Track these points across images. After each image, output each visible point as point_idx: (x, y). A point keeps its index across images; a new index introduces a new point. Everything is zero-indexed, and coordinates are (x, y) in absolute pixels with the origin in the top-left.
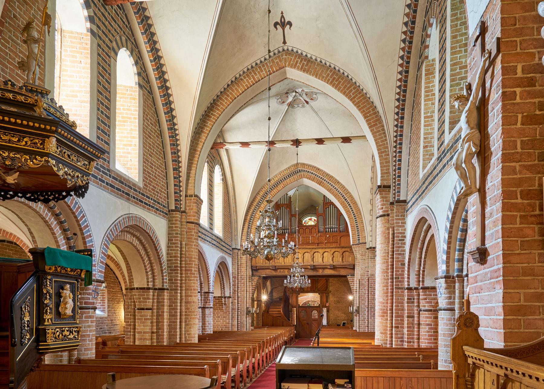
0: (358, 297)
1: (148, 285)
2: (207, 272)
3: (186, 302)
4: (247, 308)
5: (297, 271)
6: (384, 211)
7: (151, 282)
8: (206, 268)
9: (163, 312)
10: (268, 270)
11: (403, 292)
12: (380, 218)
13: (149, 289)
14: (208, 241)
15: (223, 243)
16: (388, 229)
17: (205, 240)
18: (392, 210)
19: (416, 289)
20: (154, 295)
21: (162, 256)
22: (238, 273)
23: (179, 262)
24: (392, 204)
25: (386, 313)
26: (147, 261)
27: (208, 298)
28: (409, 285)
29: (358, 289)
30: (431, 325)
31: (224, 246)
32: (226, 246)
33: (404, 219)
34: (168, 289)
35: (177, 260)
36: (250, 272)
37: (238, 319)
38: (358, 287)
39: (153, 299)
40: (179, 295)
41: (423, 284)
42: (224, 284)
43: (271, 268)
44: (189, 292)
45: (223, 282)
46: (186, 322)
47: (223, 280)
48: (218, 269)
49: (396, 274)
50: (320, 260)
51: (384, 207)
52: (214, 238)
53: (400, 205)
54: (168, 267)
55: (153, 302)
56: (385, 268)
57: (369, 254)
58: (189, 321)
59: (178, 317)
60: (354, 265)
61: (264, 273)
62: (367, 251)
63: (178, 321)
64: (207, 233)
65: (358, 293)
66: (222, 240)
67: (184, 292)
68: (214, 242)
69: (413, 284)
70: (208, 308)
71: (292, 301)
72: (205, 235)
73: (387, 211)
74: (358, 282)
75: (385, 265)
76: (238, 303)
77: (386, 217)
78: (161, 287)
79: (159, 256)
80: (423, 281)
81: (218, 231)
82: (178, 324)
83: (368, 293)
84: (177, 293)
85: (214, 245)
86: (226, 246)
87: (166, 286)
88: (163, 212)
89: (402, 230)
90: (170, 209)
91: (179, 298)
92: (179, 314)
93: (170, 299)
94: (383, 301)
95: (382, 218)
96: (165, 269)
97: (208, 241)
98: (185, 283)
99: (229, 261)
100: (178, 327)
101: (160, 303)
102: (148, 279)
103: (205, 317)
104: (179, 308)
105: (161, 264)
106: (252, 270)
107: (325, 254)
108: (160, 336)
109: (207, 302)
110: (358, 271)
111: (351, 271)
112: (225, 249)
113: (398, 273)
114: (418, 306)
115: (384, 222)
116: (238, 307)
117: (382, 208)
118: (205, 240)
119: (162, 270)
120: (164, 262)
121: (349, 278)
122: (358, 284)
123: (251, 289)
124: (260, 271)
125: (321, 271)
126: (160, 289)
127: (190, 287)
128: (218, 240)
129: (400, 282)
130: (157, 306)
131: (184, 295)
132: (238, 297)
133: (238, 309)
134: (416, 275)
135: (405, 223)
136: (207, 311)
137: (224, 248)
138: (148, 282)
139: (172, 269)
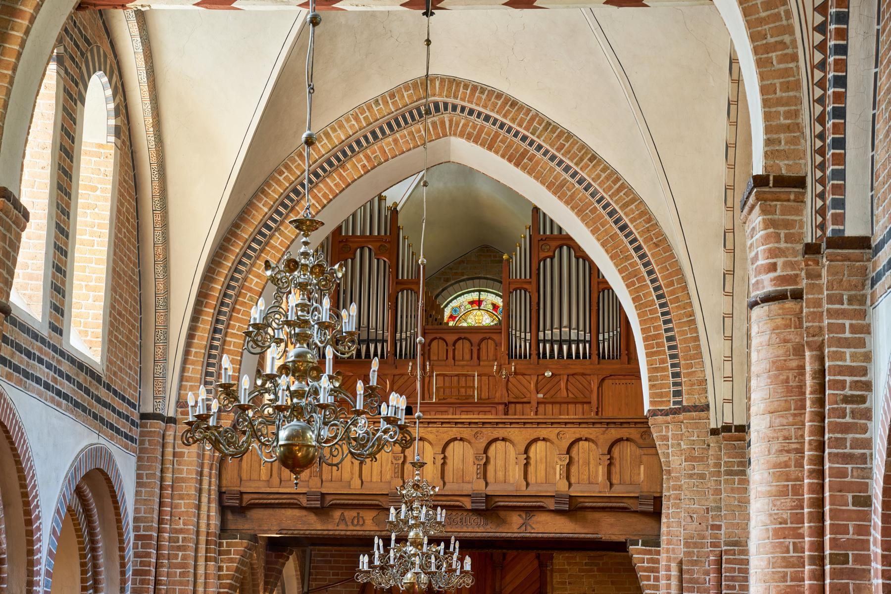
2: (28, 513)
5: (417, 518)
6: (781, 280)
8: (25, 495)
10: (289, 512)
14: (38, 381)
15: (103, 393)
16: (798, 351)
17: (27, 375)
18: (814, 275)
22: (160, 521)
24: (812, 249)
31: (106, 405)
32: (117, 403)
33: (863, 314)
42: (95, 566)
43: (304, 501)
45: (95, 558)
47: (94, 550)
48: (75, 502)
50: (515, 473)
51: (780, 262)
52: (66, 367)
53: (847, 258)
61: (274, 524)
66: (98, 379)
68: (66, 387)
73: (794, 279)
77: (789, 304)
81: (86, 337)
85: (66, 397)
86: (117, 403)
89: (853, 357)
95: (774, 306)
99: (125, 468)
107: (538, 450)
112: (112, 418)
115: (779, 321)
117: (773, 267)
118: (27, 375)
124: (256, 514)
128: (82, 378)
137: (105, 413)
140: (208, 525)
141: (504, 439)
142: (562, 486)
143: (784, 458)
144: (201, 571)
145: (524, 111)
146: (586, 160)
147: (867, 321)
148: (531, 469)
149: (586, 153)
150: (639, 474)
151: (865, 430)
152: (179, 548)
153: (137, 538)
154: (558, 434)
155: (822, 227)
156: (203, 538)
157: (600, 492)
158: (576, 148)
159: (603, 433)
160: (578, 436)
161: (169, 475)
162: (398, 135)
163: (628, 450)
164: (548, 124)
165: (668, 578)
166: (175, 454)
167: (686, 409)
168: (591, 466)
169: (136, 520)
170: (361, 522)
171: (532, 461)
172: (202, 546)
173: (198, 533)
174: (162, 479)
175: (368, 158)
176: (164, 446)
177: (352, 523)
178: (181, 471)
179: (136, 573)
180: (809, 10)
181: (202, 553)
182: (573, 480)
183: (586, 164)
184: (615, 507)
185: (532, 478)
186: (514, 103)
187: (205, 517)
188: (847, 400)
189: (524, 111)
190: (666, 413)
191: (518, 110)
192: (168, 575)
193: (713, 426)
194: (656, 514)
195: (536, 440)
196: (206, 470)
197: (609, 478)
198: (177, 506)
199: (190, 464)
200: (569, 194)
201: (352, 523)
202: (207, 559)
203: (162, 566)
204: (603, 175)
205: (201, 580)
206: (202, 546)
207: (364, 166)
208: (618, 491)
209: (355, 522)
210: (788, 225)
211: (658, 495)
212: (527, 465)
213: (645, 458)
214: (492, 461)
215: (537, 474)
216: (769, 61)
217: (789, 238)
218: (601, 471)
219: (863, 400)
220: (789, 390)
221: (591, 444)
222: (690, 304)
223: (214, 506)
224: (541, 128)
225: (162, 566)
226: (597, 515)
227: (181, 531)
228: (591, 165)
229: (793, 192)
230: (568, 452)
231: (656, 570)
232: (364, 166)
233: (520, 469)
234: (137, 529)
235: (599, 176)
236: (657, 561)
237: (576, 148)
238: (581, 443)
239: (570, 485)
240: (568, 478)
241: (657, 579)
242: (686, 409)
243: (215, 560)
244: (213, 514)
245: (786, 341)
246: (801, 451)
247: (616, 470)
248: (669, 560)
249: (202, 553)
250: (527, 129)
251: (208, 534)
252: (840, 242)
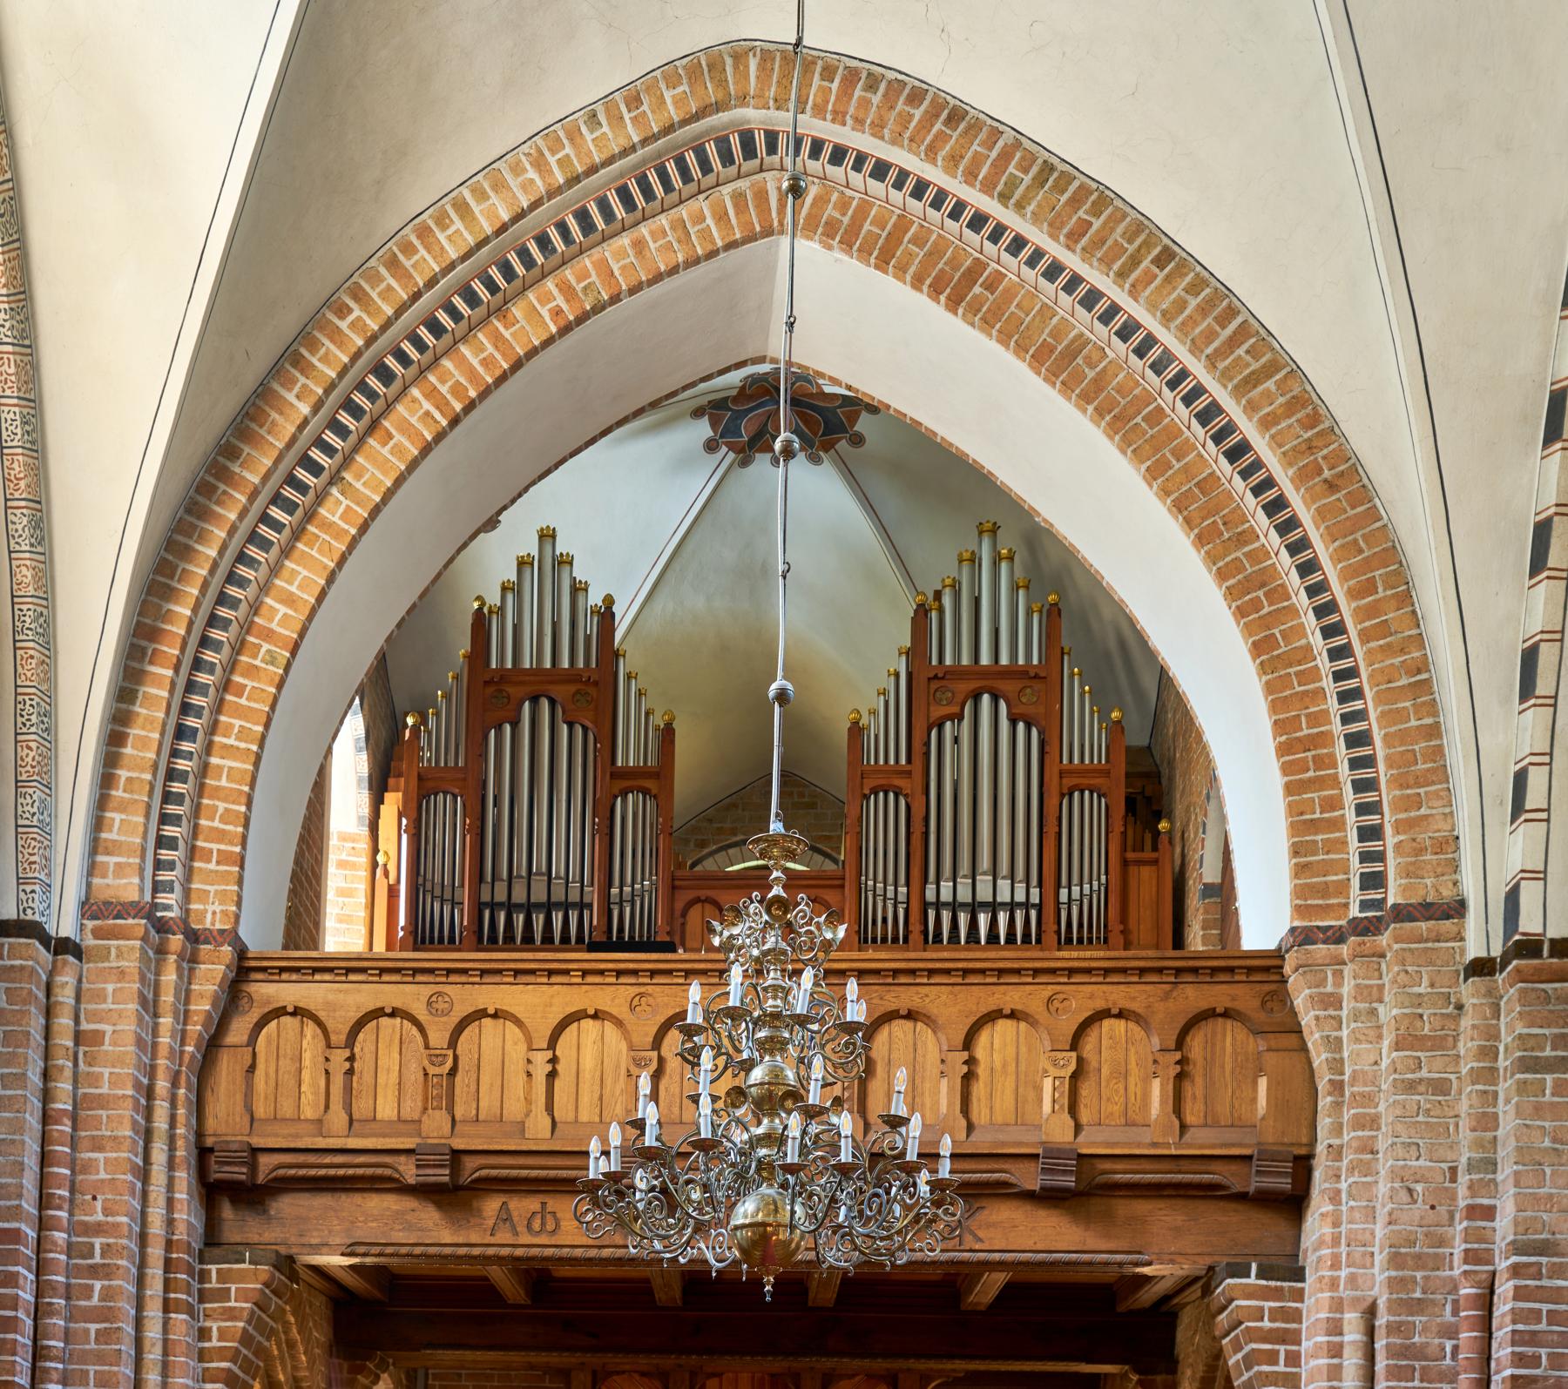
22: (44, 1201)
36: (176, 1205)
43: (409, 1171)
60: (1303, 1165)
106: (211, 1192)
107: (998, 1042)
110: (1349, 1235)
111: (1262, 1228)
121: (1244, 1295)
124: (287, 1205)
140: (170, 1223)
141: (910, 1016)
142: (1059, 1131)
144: (153, 1332)
145: (983, 135)
146: (1146, 263)
148: (979, 1090)
149: (1147, 245)
150: (1254, 1100)
152: (94, 1271)
154: (1050, 1000)
156: (156, 1252)
157: (1155, 1145)
158: (1120, 229)
159: (1166, 997)
160: (1100, 1004)
161: (64, 1086)
162: (644, 230)
163: (1230, 1037)
164: (1048, 168)
165: (1336, 1351)
166: (78, 1037)
168: (1132, 1080)
170: (550, 1226)
171: (981, 1070)
172: (155, 1272)
173: (143, 1239)
174: (47, 1096)
175: (567, 290)
176: (49, 1012)
177: (529, 1227)
178: (95, 1080)
181: (155, 1288)
182: (1085, 1116)
183: (1147, 271)
184: (1186, 1185)
186: (956, 115)
187: (162, 1201)
189: (983, 135)
191: (966, 132)
192: (67, 1336)
194: (1293, 1204)
196: (162, 1085)
197: (1178, 1110)
198: (88, 1167)
199: (119, 1060)
200: (1091, 374)
201: (529, 1227)
203: (51, 1311)
204: (1193, 302)
205: (153, 1355)
206: (155, 1272)
207: (557, 312)
208: (1202, 1141)
209: (537, 1225)
211: (1303, 1151)
212: (968, 1078)
213: (1271, 1059)
214: (880, 1069)
215: (995, 1103)
218: (1157, 1092)
221: (1131, 1025)
223: (182, 1175)
224: (1028, 179)
225: (51, 1311)
226: (1142, 1207)
227: (98, 1229)
228: (1161, 275)
230: (1074, 1046)
231: (1293, 1338)
232: (557, 312)
233: (951, 1089)
235: (1181, 305)
236: (1296, 1316)
237: (1120, 229)
238: (1106, 1023)
239: (1078, 1128)
240: (1073, 1110)
241: (1294, 1359)
243: (190, 1310)
244: (181, 1196)
247: (1195, 1089)
248: (1338, 1305)
249: (155, 1288)
250: (988, 188)
251: (169, 1245)
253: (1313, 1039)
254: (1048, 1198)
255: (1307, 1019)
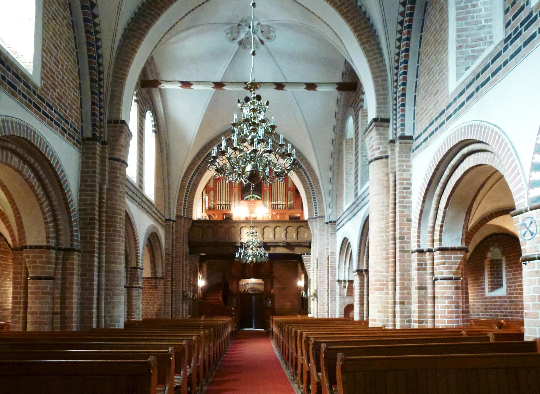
0: (315, 279)
1: (48, 242)
3: (106, 272)
4: (183, 292)
6: (382, 152)
7: (53, 238)
8: (134, 236)
9: (72, 284)
11: (409, 256)
12: (376, 162)
13: (49, 248)
16: (387, 175)
19: (430, 251)
20: (57, 258)
21: (72, 201)
22: (172, 250)
23: (97, 213)
24: (393, 142)
25: (386, 285)
26: (47, 206)
27: (135, 274)
28: (419, 246)
29: (315, 269)
30: (451, 298)
33: (409, 161)
34: (79, 251)
35: (94, 209)
36: (186, 249)
37: (172, 306)
38: (315, 266)
39: (56, 264)
40: (96, 259)
41: (440, 244)
44: (112, 256)
46: (106, 299)
49: (400, 233)
54: (80, 219)
55: (56, 269)
56: (383, 226)
57: (329, 228)
58: (112, 298)
59: (95, 292)
60: (310, 243)
62: (326, 225)
63: (95, 297)
64: (135, 191)
65: (315, 274)
67: (104, 256)
69: (426, 246)
70: (136, 287)
71: (233, 288)
72: (133, 192)
74: (315, 261)
75: (384, 222)
76: (172, 286)
77: (384, 160)
78: (68, 246)
79: (66, 199)
80: (440, 240)
82: (95, 301)
83: (328, 274)
84: (93, 256)
87: (77, 246)
88: (73, 138)
90: (85, 136)
91: (96, 264)
92: (95, 287)
93: (82, 266)
94: (382, 270)
95: (379, 161)
96: (75, 221)
97: (136, 201)
98: (106, 244)
100: (95, 306)
101: (66, 271)
102: (47, 233)
103: (131, 299)
104: (96, 278)
105: (69, 213)
107: (277, 229)
108: (64, 314)
109: (134, 281)
111: (306, 249)
113: (403, 231)
114: (433, 274)
116: (172, 291)
117: (379, 148)
119: (70, 222)
120: (74, 211)
121: (305, 257)
122: (315, 264)
123: (188, 269)
125: (272, 249)
126: (66, 250)
127: (114, 249)
129: (406, 242)
130: (63, 274)
131: (104, 260)
132: (172, 279)
133: (172, 293)
134: (430, 232)
135: (410, 166)
136: (135, 292)
138: (48, 237)
139: (87, 222)
142: (284, 239)
143: (383, 208)
144: (185, 264)
147: (410, 163)
151: (410, 198)
153: (166, 254)
155: (396, 134)
161: (174, 237)
167: (319, 217)
169: (166, 249)
172: (185, 257)
174: (172, 238)
179: (166, 264)
180: (393, 61)
185: (276, 237)
188: (405, 188)
190: (313, 219)
193: (326, 221)
194: (310, 247)
195: (277, 227)
202: (186, 260)
208: (299, 240)
210: (384, 134)
212: (275, 234)
215: (277, 236)
216: (378, 81)
217: (384, 139)
218: (295, 235)
219: (409, 188)
220: (384, 187)
222: (320, 188)
229: (386, 124)
230: (286, 229)
234: (166, 251)
240: (286, 237)
242: (319, 217)
245: (383, 172)
246: (388, 206)
252: (403, 137)
253: (311, 229)
254: (283, 246)
255: (310, 227)
